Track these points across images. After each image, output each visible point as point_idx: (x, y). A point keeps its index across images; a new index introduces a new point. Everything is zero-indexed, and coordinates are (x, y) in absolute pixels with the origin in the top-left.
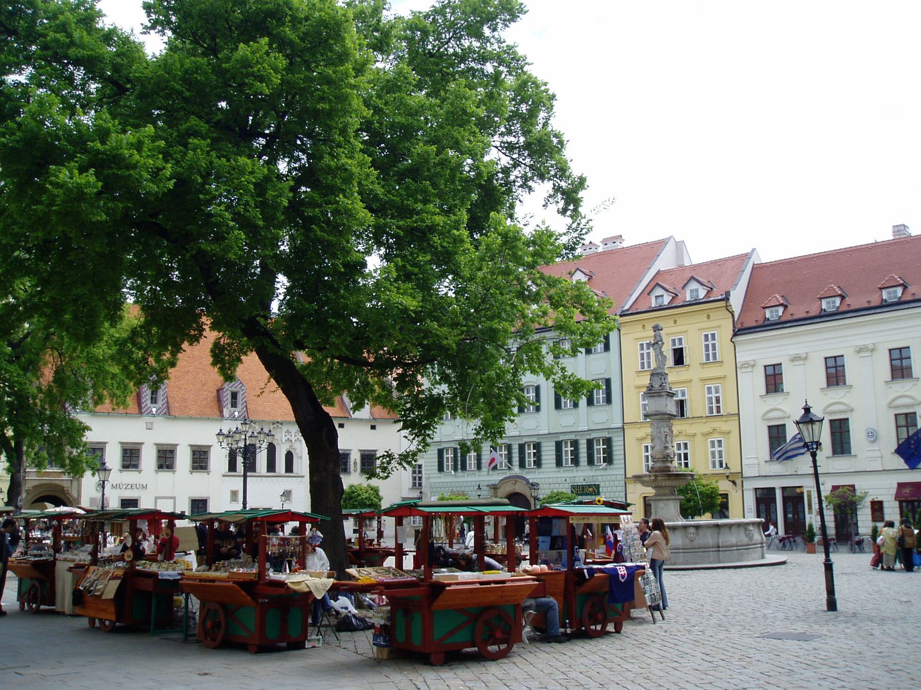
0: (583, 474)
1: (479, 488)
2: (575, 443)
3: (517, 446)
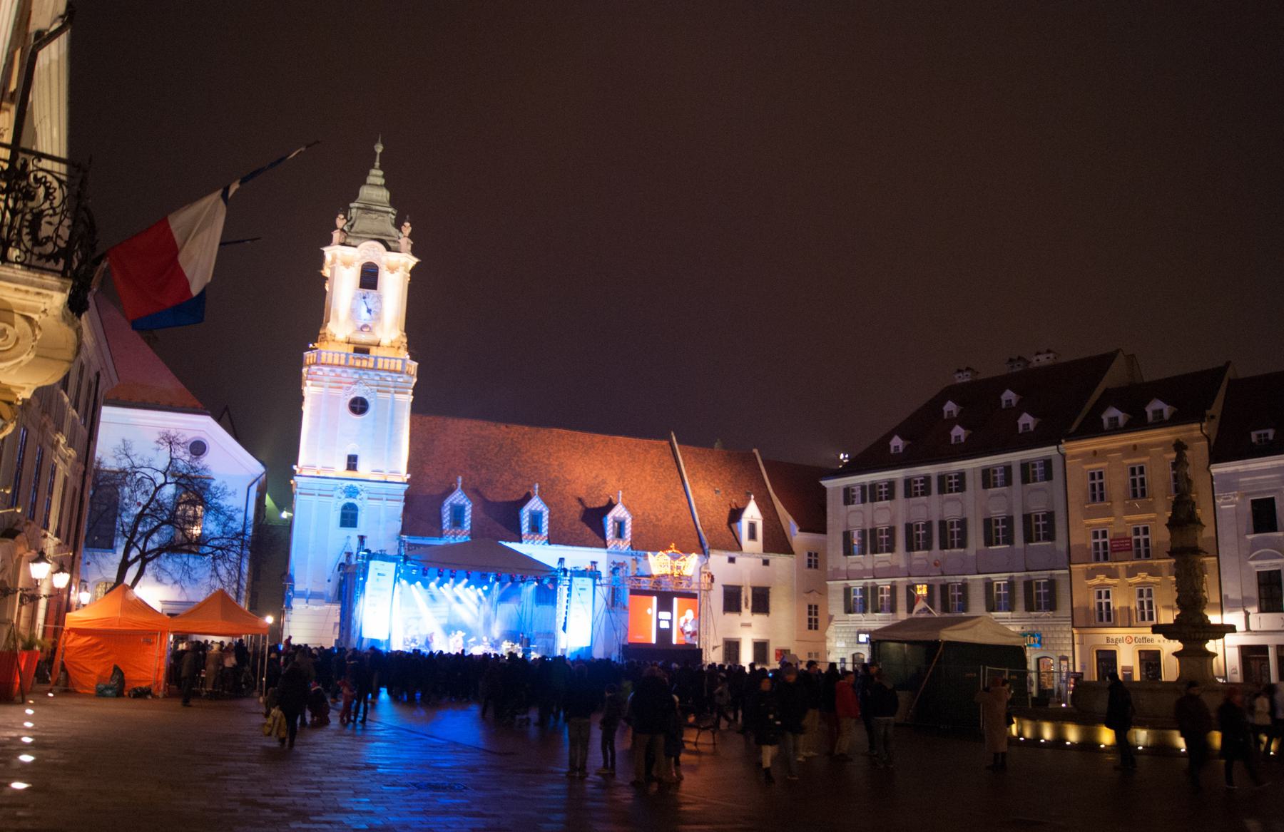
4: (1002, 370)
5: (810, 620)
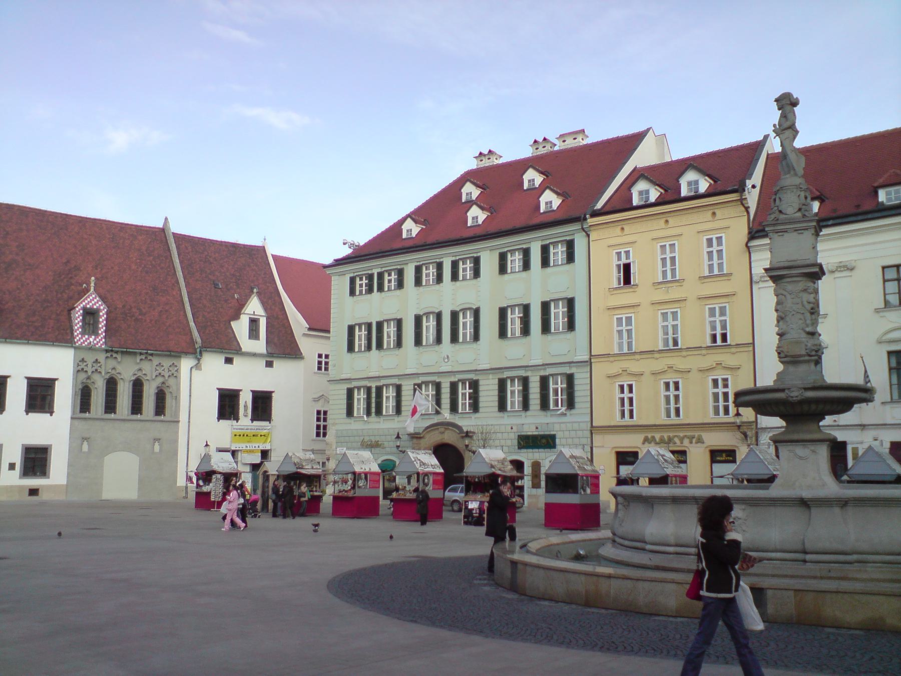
0: (534, 422)
1: (398, 437)
2: (525, 381)
3: (448, 385)
4: (527, 152)
5: (318, 427)
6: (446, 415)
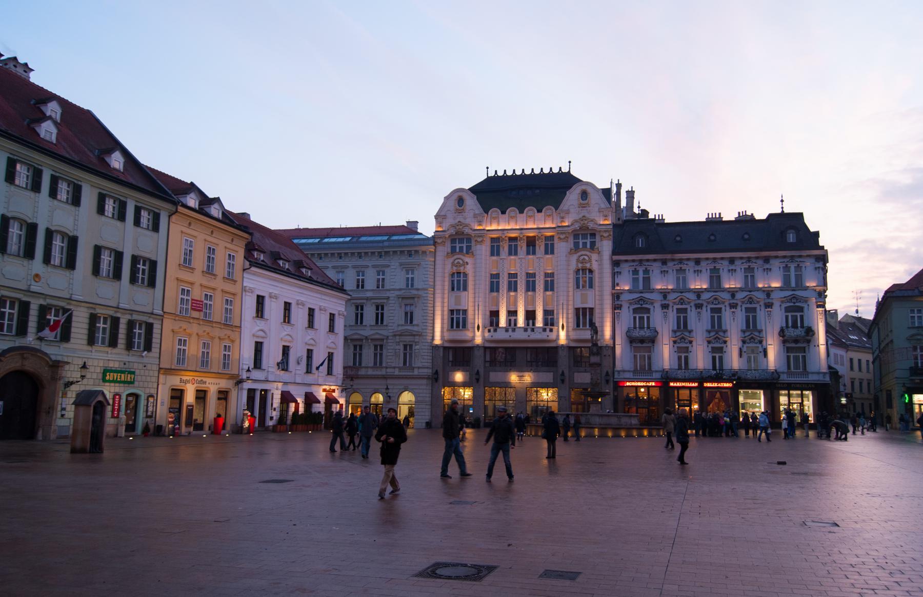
2: (115, 322)
6: (30, 339)
